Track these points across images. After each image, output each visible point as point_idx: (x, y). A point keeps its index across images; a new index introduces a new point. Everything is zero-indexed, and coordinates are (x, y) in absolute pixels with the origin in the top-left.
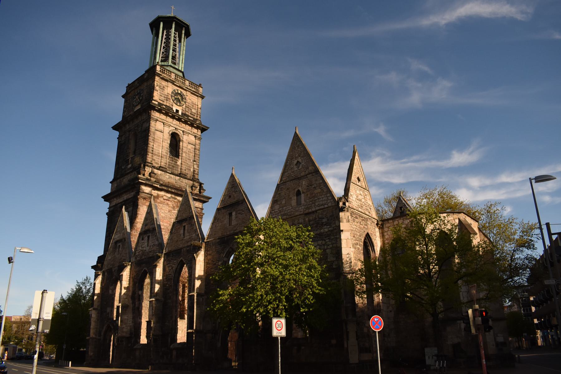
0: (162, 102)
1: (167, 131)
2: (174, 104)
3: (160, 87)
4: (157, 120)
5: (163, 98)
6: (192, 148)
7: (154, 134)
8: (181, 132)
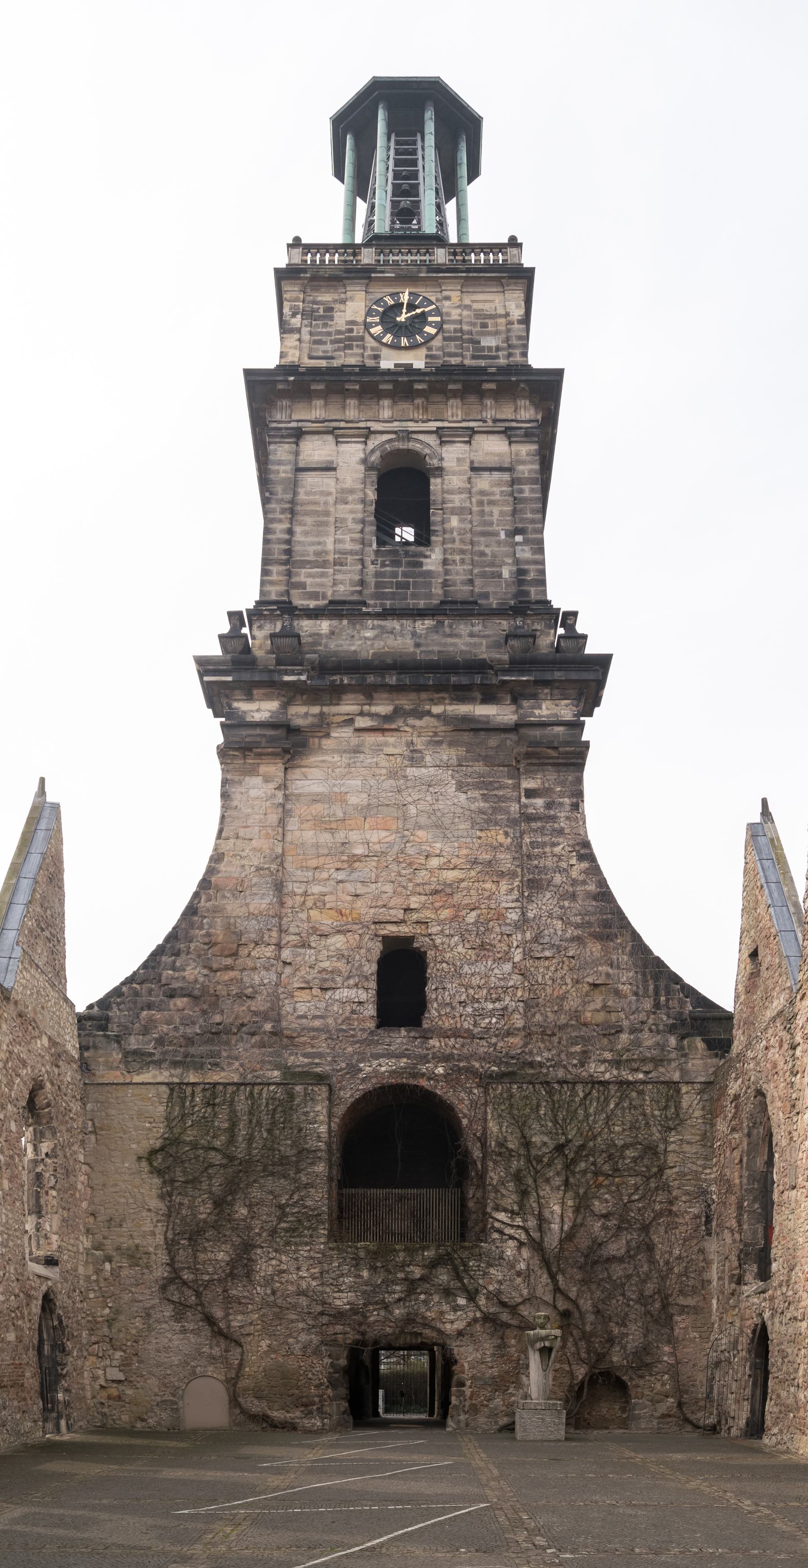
0: (323, 363)
1: (351, 457)
2: (385, 352)
3: (309, 315)
4: (298, 434)
5: (329, 347)
6: (499, 484)
7: (294, 485)
8: (432, 440)
